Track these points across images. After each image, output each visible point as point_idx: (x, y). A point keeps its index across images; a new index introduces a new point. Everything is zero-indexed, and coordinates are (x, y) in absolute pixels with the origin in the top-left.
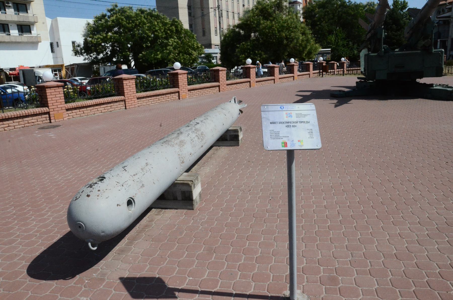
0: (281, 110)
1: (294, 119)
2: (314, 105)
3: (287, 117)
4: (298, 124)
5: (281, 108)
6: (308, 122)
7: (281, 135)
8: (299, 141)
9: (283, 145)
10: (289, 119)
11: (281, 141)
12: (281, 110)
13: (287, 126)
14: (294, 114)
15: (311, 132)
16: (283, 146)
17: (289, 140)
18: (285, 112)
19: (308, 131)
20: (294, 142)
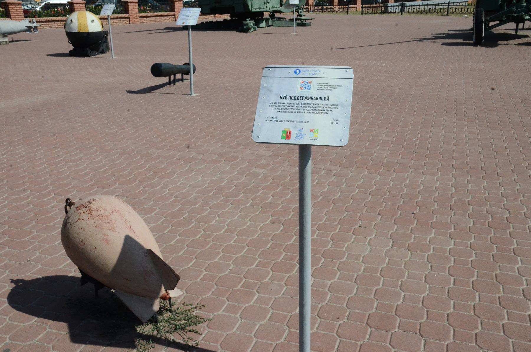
0: (295, 76)
2: (352, 71)
5: (295, 72)
8: (311, 131)
9: (285, 135)
10: (306, 93)
12: (295, 76)
14: (314, 83)
16: (282, 138)
17: (295, 127)
18: (300, 80)
20: (304, 132)
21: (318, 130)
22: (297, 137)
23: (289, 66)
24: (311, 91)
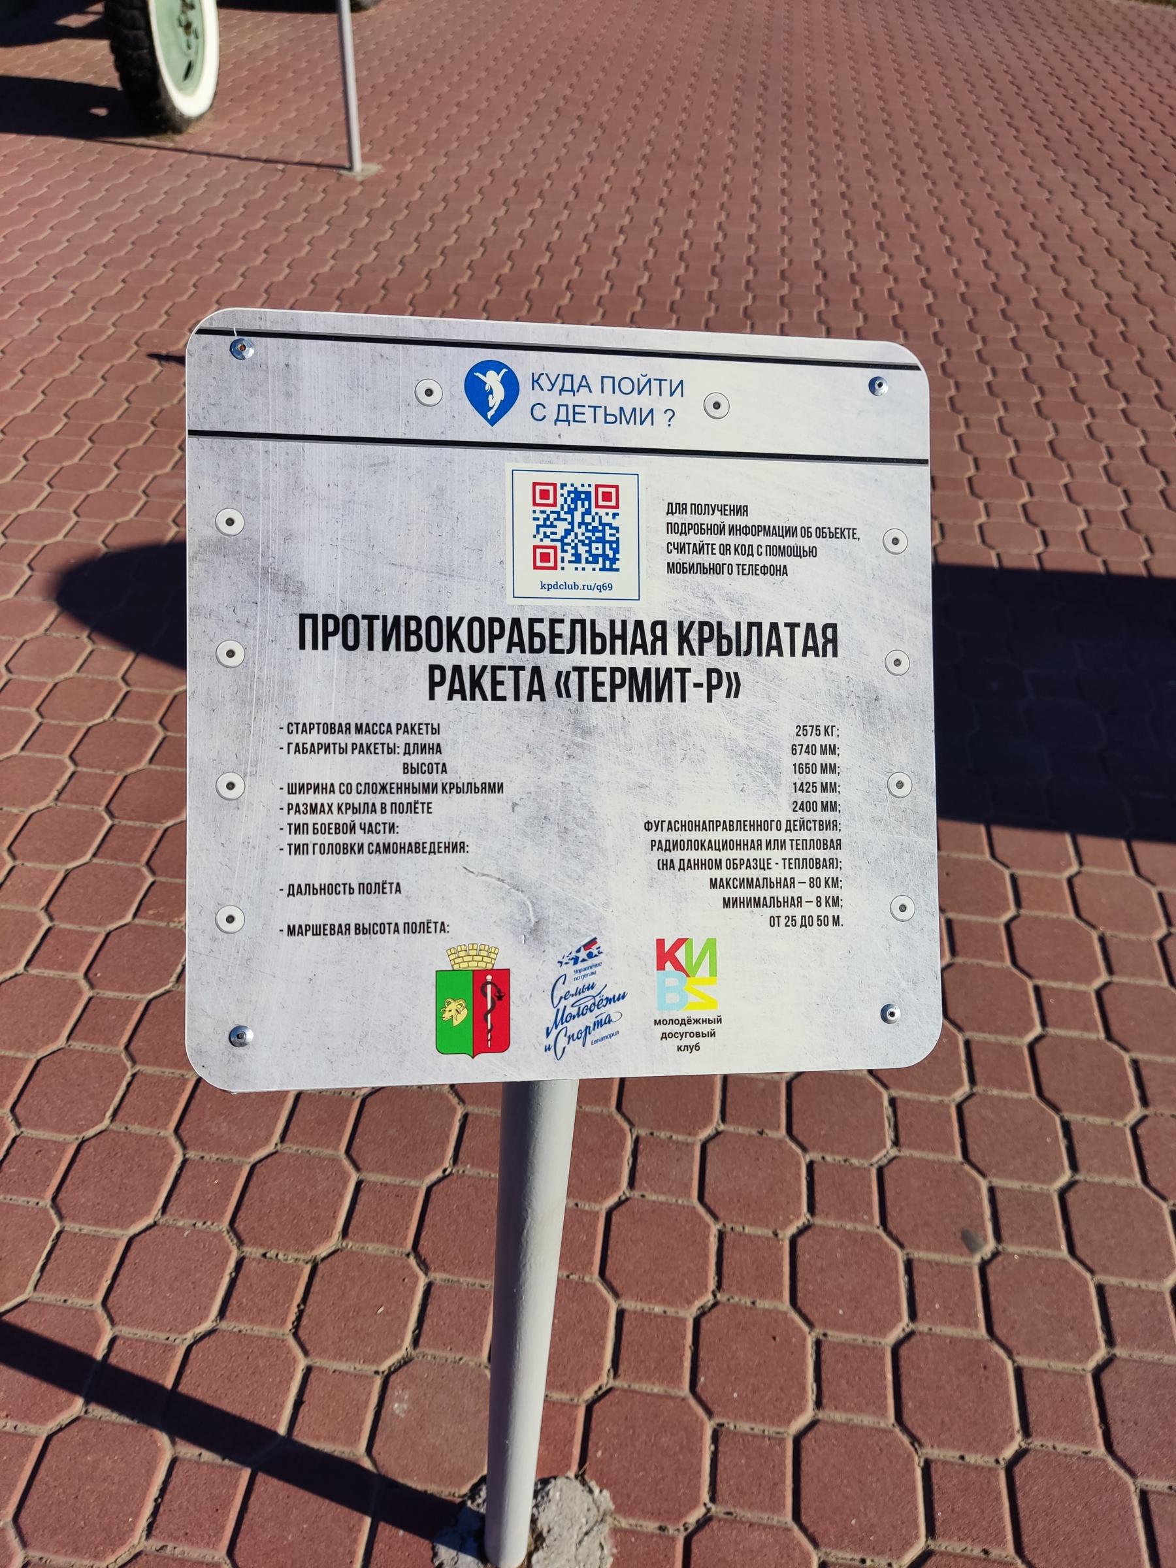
0: (475, 427)
3: (543, 559)
5: (476, 392)
8: (666, 956)
9: (459, 1013)
12: (475, 427)
17: (535, 932)
21: (710, 945)
22: (561, 1019)
24: (623, 580)
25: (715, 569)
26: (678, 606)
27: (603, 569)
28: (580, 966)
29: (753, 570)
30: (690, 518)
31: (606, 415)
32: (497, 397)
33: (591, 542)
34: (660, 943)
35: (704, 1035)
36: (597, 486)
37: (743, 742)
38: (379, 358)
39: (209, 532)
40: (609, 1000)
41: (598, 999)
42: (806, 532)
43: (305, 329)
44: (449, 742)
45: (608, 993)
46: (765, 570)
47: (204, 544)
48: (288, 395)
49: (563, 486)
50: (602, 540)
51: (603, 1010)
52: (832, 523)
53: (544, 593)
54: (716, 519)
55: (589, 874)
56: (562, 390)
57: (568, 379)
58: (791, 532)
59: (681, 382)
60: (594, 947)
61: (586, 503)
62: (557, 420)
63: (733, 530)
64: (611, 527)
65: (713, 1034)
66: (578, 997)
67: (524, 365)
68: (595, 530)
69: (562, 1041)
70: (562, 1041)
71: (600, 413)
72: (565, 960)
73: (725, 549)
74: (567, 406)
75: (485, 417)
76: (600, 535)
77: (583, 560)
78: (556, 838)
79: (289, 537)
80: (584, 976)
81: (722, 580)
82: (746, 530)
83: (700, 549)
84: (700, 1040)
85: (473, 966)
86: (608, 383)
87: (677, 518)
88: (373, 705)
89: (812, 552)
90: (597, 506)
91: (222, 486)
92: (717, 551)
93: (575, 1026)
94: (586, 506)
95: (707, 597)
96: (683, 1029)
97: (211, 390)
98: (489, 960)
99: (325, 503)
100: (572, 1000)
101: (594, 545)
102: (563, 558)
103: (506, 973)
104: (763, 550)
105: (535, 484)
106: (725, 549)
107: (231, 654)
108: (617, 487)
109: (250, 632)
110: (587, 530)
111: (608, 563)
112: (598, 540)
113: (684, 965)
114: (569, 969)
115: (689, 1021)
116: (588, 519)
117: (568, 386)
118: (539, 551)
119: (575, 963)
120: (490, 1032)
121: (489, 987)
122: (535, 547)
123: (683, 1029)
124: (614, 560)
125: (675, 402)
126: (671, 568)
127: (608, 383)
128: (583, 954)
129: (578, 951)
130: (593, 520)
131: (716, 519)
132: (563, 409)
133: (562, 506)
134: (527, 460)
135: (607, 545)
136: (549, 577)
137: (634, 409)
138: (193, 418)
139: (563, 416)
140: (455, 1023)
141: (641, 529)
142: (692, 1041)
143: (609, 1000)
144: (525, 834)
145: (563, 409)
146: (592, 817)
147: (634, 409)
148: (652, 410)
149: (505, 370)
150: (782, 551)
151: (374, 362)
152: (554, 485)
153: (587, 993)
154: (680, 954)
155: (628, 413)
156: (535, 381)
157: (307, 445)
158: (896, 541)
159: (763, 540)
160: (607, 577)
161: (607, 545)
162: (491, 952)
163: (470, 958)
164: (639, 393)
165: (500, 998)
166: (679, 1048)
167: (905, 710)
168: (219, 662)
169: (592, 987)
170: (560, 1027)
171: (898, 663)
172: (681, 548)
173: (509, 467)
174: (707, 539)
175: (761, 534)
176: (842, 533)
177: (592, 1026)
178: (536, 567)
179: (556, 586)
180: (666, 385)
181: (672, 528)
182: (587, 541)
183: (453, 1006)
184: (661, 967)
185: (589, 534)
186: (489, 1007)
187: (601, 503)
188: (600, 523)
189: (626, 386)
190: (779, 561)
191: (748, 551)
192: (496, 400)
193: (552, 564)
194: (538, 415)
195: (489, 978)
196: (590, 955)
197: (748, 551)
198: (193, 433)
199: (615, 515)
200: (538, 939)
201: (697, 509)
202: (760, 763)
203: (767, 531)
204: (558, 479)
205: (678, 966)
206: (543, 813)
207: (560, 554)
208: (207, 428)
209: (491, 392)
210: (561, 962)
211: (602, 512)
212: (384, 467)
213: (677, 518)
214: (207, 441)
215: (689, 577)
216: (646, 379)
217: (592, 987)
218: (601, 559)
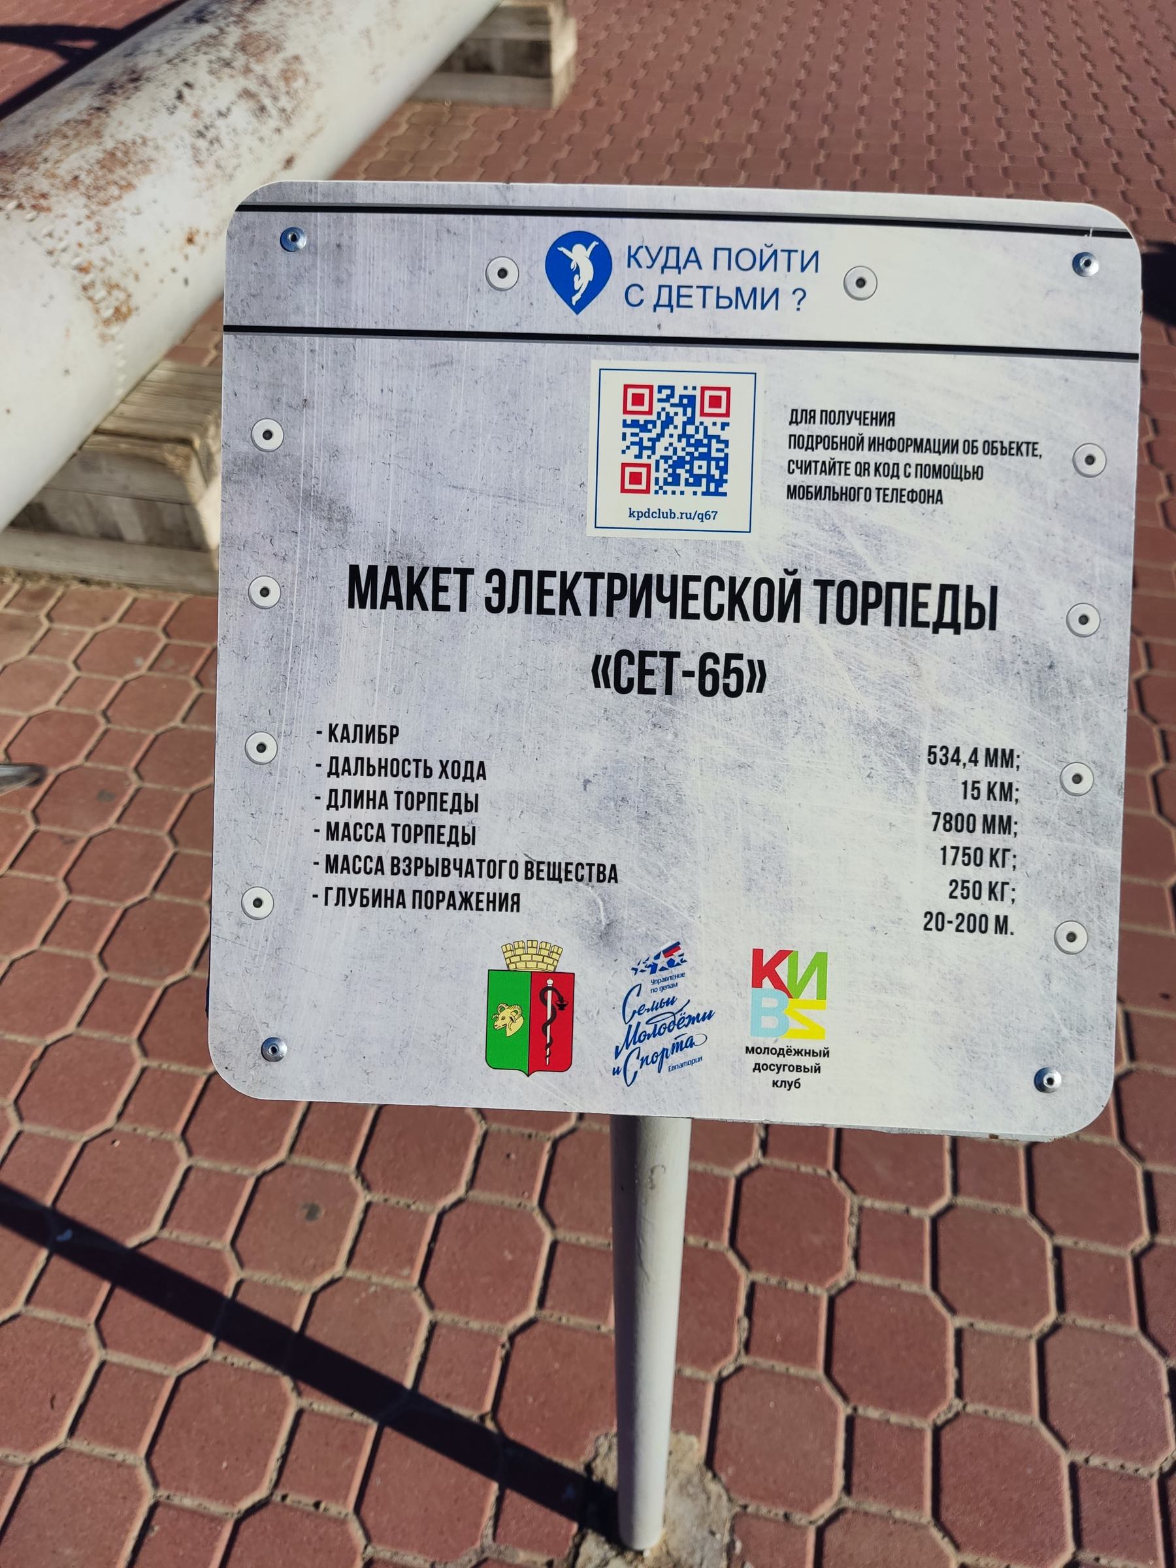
1: (755, 526)
3: (633, 480)
4: (803, 649)
5: (559, 272)
6: (969, 611)
7: (498, 835)
8: (764, 970)
9: (514, 1022)
10: (677, 537)
11: (483, 943)
13: (603, 672)
15: (979, 828)
16: (497, 1054)
17: (606, 935)
19: (946, 789)
20: (694, 989)
21: (820, 961)
22: (634, 1038)
23: (486, 192)
24: (729, 508)
25: (850, 494)
26: (798, 541)
27: (707, 493)
28: (659, 975)
29: (898, 495)
30: (819, 429)
31: (718, 297)
32: (586, 275)
33: (693, 458)
34: (758, 954)
35: (806, 1070)
36: (703, 389)
37: (873, 715)
38: (445, 234)
39: (245, 448)
40: (692, 1020)
41: (678, 1017)
42: (971, 447)
43: (361, 199)
44: (513, 703)
45: (691, 1011)
46: (914, 496)
47: (239, 462)
48: (338, 281)
49: (661, 388)
50: (706, 457)
51: (684, 1030)
52: (1006, 433)
53: (633, 522)
54: (853, 429)
55: (674, 870)
56: (665, 267)
57: (673, 253)
58: (951, 446)
59: (816, 254)
60: (676, 954)
61: (689, 410)
62: (657, 305)
63: (875, 444)
64: (719, 441)
65: (818, 1069)
66: (655, 1013)
67: (618, 236)
68: (699, 443)
69: (634, 1064)
70: (634, 1064)
71: (711, 295)
72: (642, 967)
73: (863, 469)
74: (670, 287)
75: (569, 302)
76: (704, 450)
77: (682, 482)
78: (634, 825)
79: (335, 454)
80: (663, 988)
81: (855, 509)
82: (891, 445)
83: (830, 468)
84: (801, 1075)
85: (532, 965)
86: (723, 256)
87: (803, 429)
88: (426, 657)
89: (977, 473)
90: (703, 414)
91: (261, 392)
92: (851, 471)
93: (651, 1047)
94: (689, 414)
95: (835, 530)
96: (780, 1060)
97: (251, 278)
98: (550, 961)
99: (377, 413)
100: (646, 1016)
101: (696, 463)
102: (657, 479)
103: (569, 978)
104: (912, 470)
105: (626, 387)
106: (863, 469)
107: (265, 592)
108: (728, 390)
109: (289, 566)
110: (689, 444)
111: (712, 486)
112: (702, 457)
113: (786, 984)
114: (646, 978)
115: (789, 1052)
116: (690, 430)
117: (672, 262)
118: (628, 470)
119: (653, 972)
120: (549, 1047)
121: (550, 992)
122: (624, 466)
123: (780, 1060)
124: (721, 482)
125: (808, 279)
126: (792, 492)
127: (723, 256)
128: (663, 961)
129: (657, 957)
130: (697, 431)
131: (853, 429)
132: (665, 291)
133: (659, 414)
134: (619, 357)
135: (713, 463)
136: (640, 502)
137: (754, 290)
138: (231, 313)
139: (664, 300)
140: (509, 1033)
141: (757, 443)
142: (791, 1076)
143: (692, 1020)
144: (598, 818)
145: (665, 291)
146: (679, 800)
147: (754, 290)
148: (776, 291)
149: (595, 244)
150: (938, 472)
151: (438, 238)
152: (651, 388)
153: (666, 1009)
154: (782, 970)
155: (746, 294)
156: (632, 257)
157: (360, 342)
158: (1090, 460)
159: (914, 457)
160: (712, 503)
161: (713, 463)
162: (554, 952)
163: (528, 958)
164: (762, 268)
165: (562, 1007)
166: (775, 1084)
167: (1088, 682)
168: (253, 602)
169: (671, 1002)
170: (632, 1047)
171: (1084, 620)
172: (806, 467)
173: (596, 365)
174: (840, 455)
175: (911, 449)
176: (1019, 449)
177: (670, 1047)
178: (623, 490)
179: (648, 514)
180: (796, 257)
181: (796, 441)
182: (688, 458)
183: (507, 1012)
184: (757, 983)
185: (691, 449)
186: (549, 1017)
187: (707, 410)
188: (706, 435)
189: (746, 260)
190: (932, 484)
191: (892, 471)
192: (581, 282)
193: (643, 486)
194: (634, 299)
195: (550, 982)
196: (671, 964)
197: (892, 471)
198: (229, 329)
199: (724, 425)
200: (608, 944)
201: (829, 417)
202: (894, 742)
203: (919, 445)
204: (656, 380)
205: (778, 984)
206: (620, 793)
207: (654, 475)
208: (246, 323)
209: (578, 271)
210: (636, 970)
211: (708, 421)
212: (447, 367)
213: (803, 429)
214: (246, 338)
215: (814, 504)
216: (771, 250)
217: (671, 1002)
218: (704, 481)
